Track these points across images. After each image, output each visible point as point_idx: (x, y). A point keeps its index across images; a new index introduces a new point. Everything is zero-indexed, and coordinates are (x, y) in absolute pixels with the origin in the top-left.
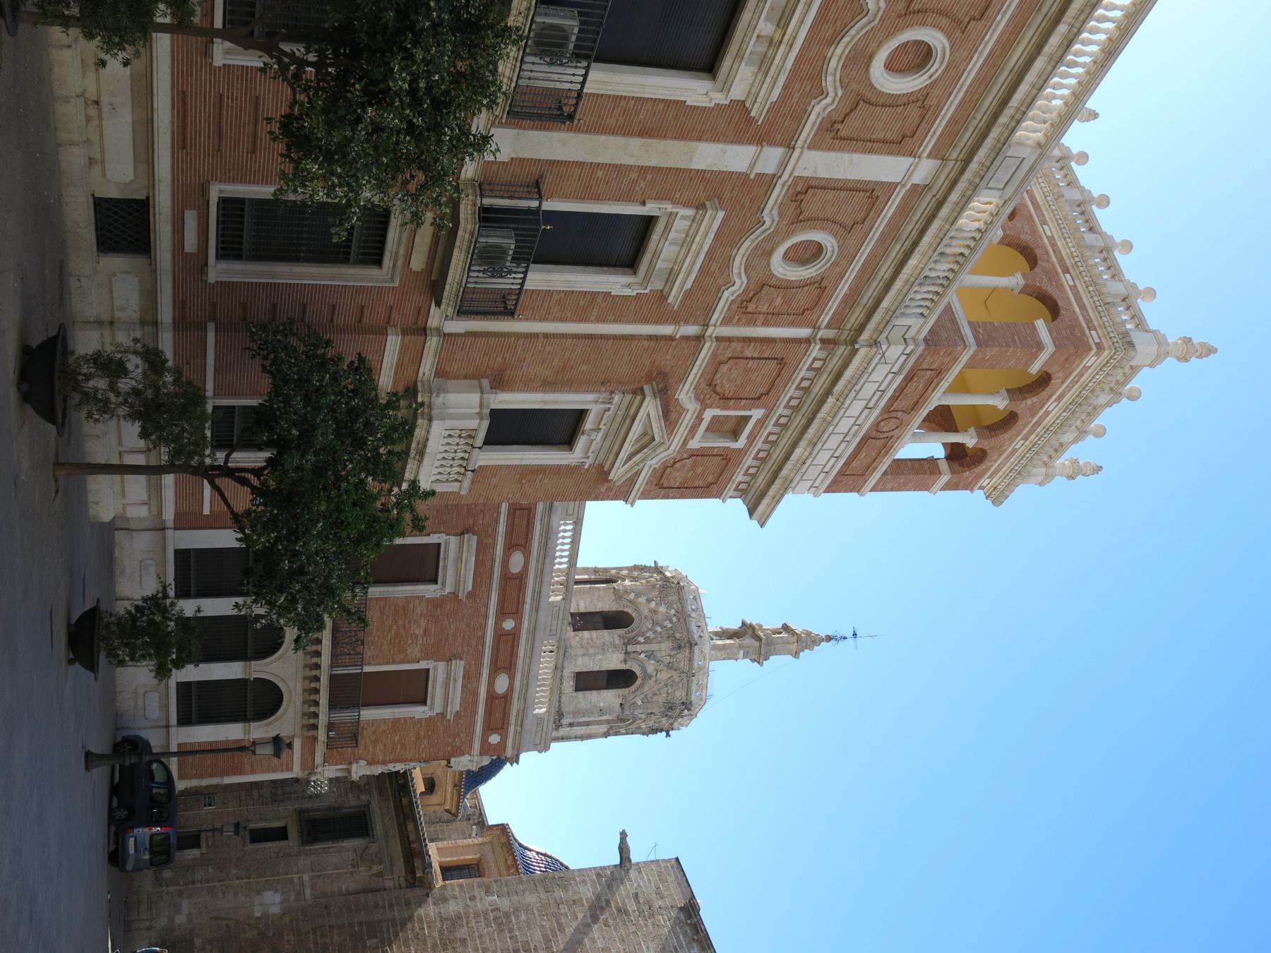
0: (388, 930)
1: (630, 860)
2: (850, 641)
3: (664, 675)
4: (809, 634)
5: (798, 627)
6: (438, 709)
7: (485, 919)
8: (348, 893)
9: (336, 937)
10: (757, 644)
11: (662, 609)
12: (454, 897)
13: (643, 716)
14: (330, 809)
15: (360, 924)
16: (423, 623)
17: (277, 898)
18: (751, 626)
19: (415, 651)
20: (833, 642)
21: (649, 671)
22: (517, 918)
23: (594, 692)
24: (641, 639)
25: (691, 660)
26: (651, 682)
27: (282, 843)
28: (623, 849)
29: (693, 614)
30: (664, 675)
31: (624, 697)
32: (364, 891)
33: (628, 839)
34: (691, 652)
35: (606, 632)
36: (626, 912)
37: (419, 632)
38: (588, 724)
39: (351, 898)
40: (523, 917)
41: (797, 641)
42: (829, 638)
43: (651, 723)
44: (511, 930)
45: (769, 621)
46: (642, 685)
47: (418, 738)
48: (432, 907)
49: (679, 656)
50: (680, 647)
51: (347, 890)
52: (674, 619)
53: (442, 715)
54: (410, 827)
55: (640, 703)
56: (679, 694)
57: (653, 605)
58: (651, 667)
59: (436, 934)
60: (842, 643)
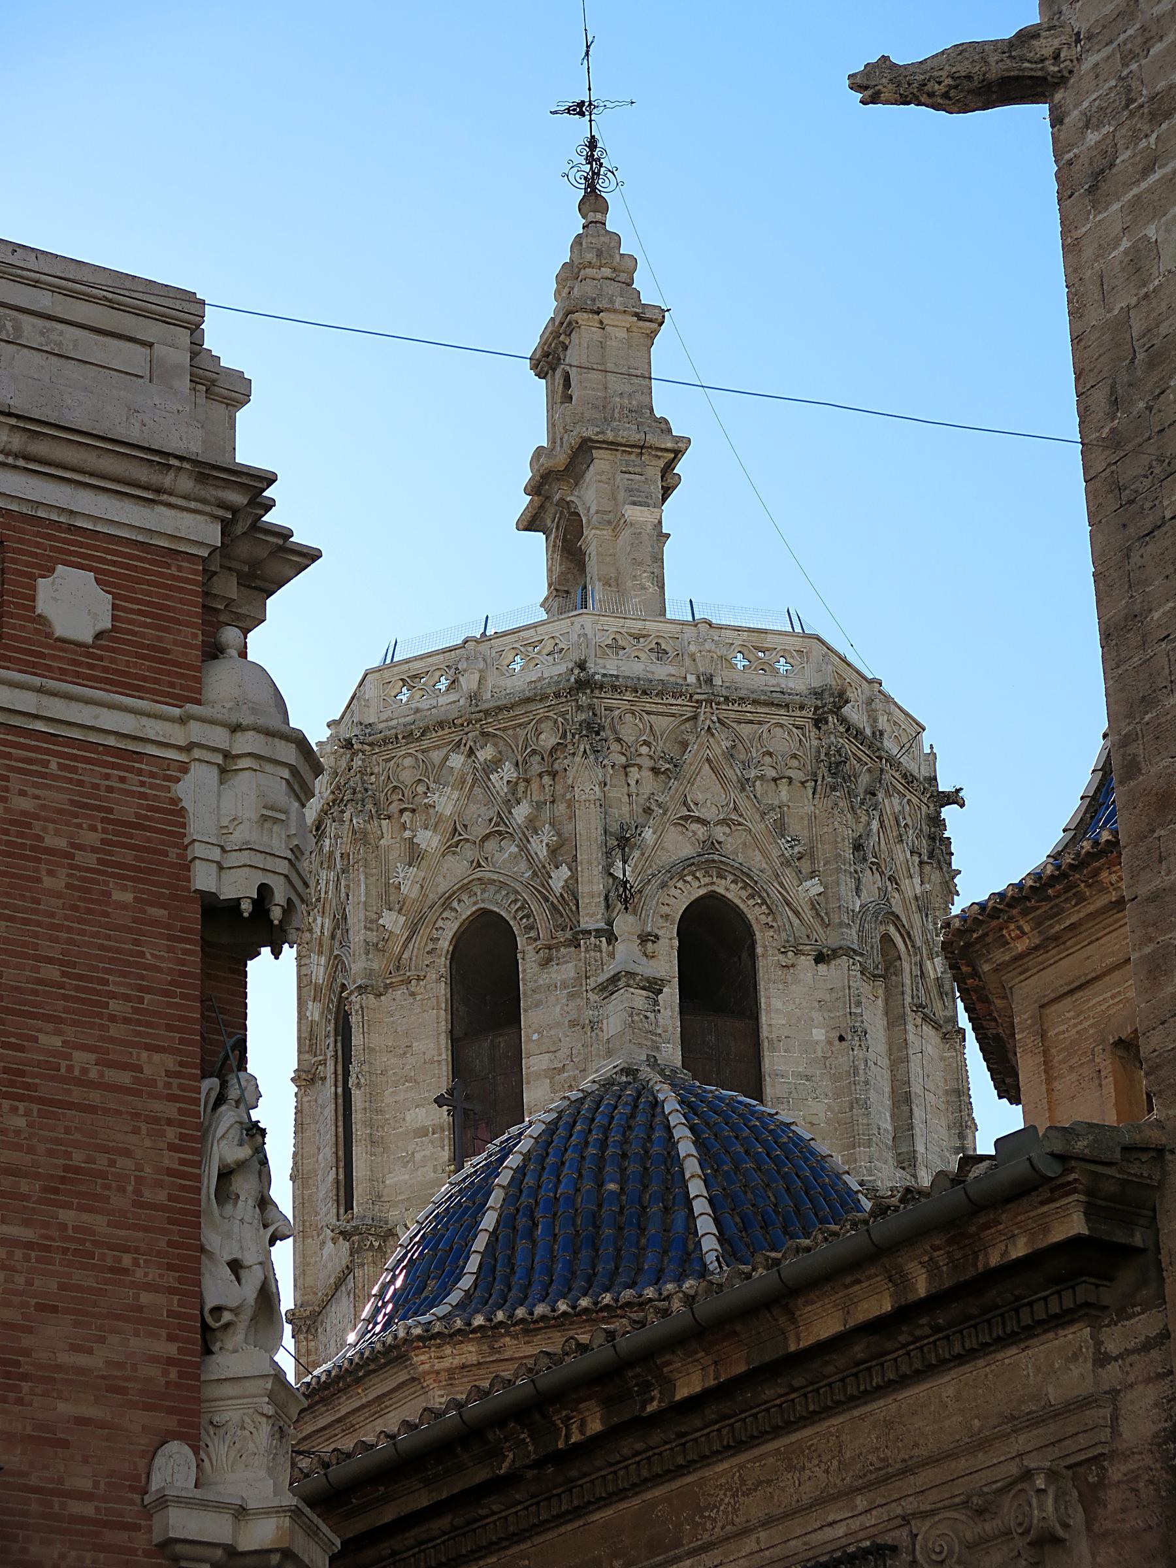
1: (1026, 36)
2: (605, 126)
4: (570, 275)
10: (602, 462)
11: (445, 802)
13: (872, 882)
18: (539, 487)
20: (605, 186)
21: (688, 850)
24: (559, 877)
26: (732, 842)
28: (971, 82)
29: (469, 682)
33: (909, 52)
34: (615, 686)
35: (529, 1019)
38: (902, 1099)
42: (593, 202)
43: (901, 854)
45: (522, 419)
46: (743, 876)
49: (628, 732)
50: (592, 729)
52: (486, 753)
55: (813, 887)
56: (782, 738)
57: (429, 840)
58: (680, 845)
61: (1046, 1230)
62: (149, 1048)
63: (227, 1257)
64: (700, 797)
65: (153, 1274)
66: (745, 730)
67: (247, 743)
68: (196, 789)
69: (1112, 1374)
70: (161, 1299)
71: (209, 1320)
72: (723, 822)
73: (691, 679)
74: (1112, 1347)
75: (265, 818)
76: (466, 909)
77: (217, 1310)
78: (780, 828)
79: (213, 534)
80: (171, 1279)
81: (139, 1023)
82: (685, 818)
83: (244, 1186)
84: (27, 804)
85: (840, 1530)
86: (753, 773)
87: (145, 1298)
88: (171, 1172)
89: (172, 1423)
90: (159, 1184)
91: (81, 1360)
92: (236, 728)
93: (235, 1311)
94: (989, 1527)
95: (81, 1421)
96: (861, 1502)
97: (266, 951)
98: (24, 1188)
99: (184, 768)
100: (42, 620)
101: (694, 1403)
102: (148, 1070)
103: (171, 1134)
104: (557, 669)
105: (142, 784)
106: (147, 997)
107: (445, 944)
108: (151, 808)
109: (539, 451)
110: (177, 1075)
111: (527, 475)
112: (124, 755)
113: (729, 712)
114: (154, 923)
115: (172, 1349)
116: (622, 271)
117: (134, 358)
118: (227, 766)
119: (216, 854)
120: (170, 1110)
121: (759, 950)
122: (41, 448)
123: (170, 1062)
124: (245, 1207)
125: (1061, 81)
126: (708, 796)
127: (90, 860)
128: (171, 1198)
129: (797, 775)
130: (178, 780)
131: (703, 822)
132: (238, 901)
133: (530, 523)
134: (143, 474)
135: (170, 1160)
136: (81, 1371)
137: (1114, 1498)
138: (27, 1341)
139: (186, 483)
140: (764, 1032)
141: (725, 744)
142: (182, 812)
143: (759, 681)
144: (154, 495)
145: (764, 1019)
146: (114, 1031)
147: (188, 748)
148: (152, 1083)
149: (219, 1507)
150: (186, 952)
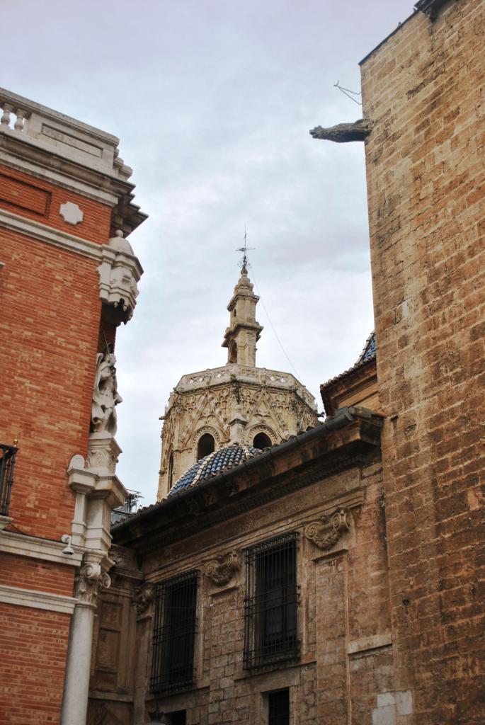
0: (453, 474)
1: (359, 122)
5: (257, 352)
8: (384, 564)
9: (463, 573)
12: (400, 373)
14: (247, 617)
15: (439, 529)
17: (385, 699)
18: (227, 337)
20: (247, 268)
22: (439, 256)
26: (268, 422)
27: (293, 698)
32: (382, 536)
33: (329, 124)
36: (437, 94)
39: (393, 555)
40: (439, 247)
41: (244, 296)
42: (244, 272)
44: (460, 259)
45: (225, 321)
46: (270, 429)
47: (38, 344)
48: (414, 407)
51: (379, 567)
54: (282, 468)
59: (463, 385)
60: (249, 260)
61: (348, 438)
62: (81, 340)
63: (100, 404)
65: (76, 405)
66: (272, 395)
67: (121, 258)
68: (104, 269)
69: (365, 482)
70: (79, 413)
71: (93, 422)
72: (265, 416)
74: (365, 474)
75: (123, 280)
76: (203, 433)
77: (96, 419)
78: (279, 418)
79: (116, 201)
80: (82, 407)
81: (79, 333)
83: (109, 386)
84: (51, 266)
85: (283, 529)
86: (274, 405)
87: (73, 412)
88: (85, 377)
89: (78, 449)
90: (81, 380)
91: (52, 427)
92: (117, 254)
93: (102, 420)
94: (327, 526)
95: (49, 445)
96: (290, 521)
97: (122, 323)
98: (38, 374)
99: (101, 263)
100: (61, 216)
101: (244, 493)
102: (81, 346)
103: (86, 366)
104: (227, 378)
105: (87, 266)
106: (83, 326)
107: (197, 441)
108: (89, 273)
109: (228, 328)
110: (90, 349)
111: (224, 333)
112: (84, 256)
114: (87, 305)
115: (80, 428)
116: (250, 287)
117: (97, 151)
118: (114, 265)
119: (108, 288)
120: (87, 359)
122: (65, 167)
123: (88, 345)
124: (108, 392)
125: (368, 134)
126: (263, 410)
127: (69, 284)
128: (84, 384)
129: (284, 407)
130: (98, 266)
131: (261, 416)
132: (114, 302)
133: (225, 345)
134: (95, 179)
135: (85, 373)
136: (51, 431)
137: (364, 517)
138: (34, 419)
139: (107, 184)
141: (268, 398)
142: (99, 276)
143: (277, 384)
144: (98, 187)
146: (71, 333)
147: (102, 258)
148: (81, 350)
149: (90, 475)
150: (96, 315)
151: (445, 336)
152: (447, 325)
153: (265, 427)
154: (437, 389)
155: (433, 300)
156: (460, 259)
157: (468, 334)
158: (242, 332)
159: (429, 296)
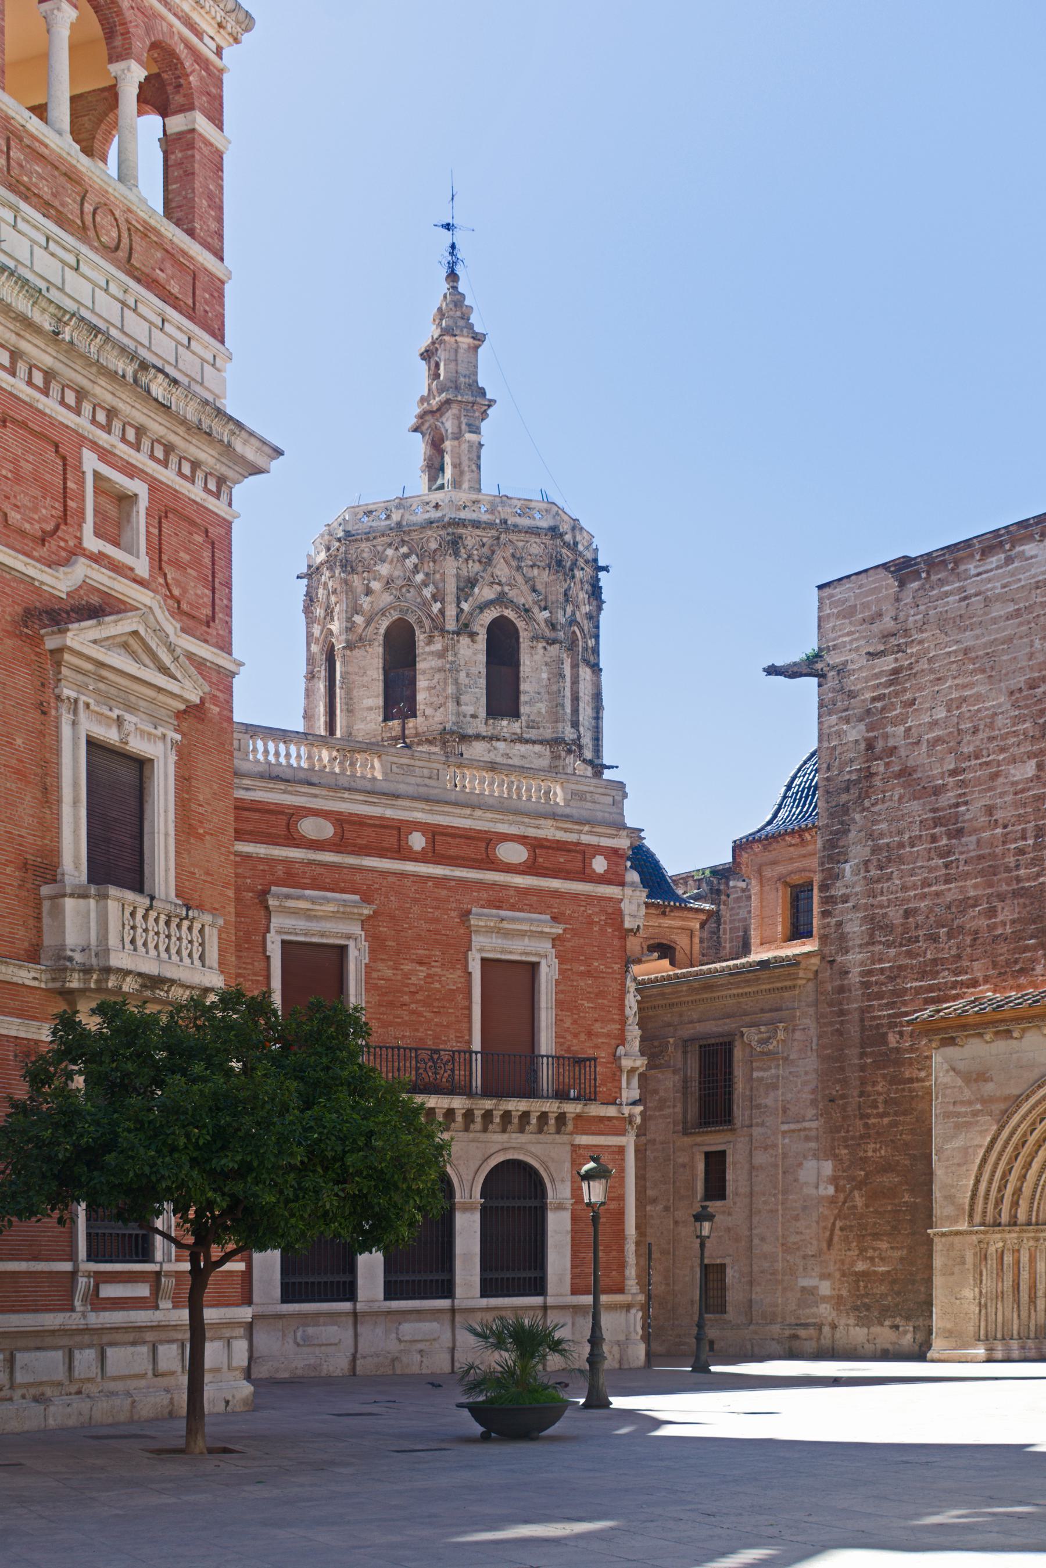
3: (502, 570)
6: (546, 946)
7: (878, 881)
16: (407, 967)
19: (452, 978)
23: (523, 686)
25: (476, 524)
26: (512, 594)
30: (502, 570)
31: (535, 638)
37: (422, 972)
46: (516, 607)
49: (470, 542)
53: (556, 940)
55: (546, 614)
64: (499, 573)
66: (521, 544)
73: (498, 521)
78: (534, 590)
82: (492, 583)
113: (513, 537)
121: (521, 640)
140: (522, 674)
145: (522, 668)
151: (882, 907)
152: (885, 898)
153: (510, 603)
154: (871, 948)
155: (874, 872)
156: (901, 845)
157: (901, 912)
158: (453, 407)
159: (871, 867)
